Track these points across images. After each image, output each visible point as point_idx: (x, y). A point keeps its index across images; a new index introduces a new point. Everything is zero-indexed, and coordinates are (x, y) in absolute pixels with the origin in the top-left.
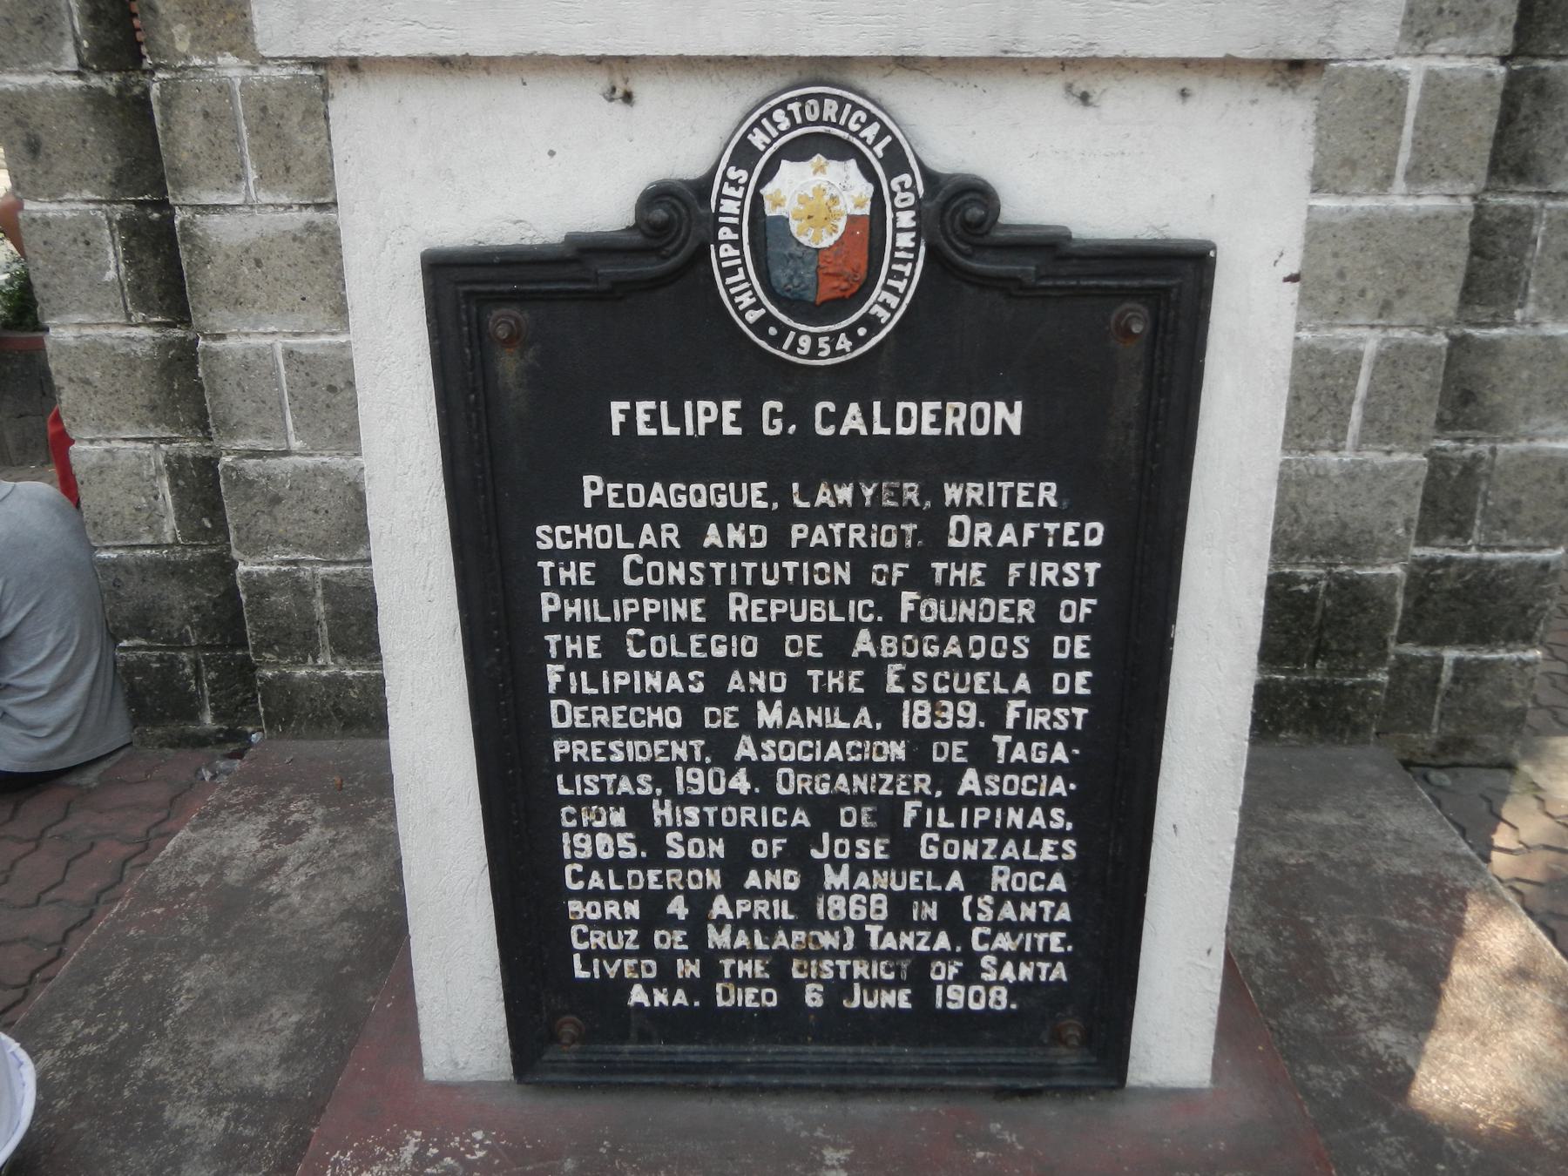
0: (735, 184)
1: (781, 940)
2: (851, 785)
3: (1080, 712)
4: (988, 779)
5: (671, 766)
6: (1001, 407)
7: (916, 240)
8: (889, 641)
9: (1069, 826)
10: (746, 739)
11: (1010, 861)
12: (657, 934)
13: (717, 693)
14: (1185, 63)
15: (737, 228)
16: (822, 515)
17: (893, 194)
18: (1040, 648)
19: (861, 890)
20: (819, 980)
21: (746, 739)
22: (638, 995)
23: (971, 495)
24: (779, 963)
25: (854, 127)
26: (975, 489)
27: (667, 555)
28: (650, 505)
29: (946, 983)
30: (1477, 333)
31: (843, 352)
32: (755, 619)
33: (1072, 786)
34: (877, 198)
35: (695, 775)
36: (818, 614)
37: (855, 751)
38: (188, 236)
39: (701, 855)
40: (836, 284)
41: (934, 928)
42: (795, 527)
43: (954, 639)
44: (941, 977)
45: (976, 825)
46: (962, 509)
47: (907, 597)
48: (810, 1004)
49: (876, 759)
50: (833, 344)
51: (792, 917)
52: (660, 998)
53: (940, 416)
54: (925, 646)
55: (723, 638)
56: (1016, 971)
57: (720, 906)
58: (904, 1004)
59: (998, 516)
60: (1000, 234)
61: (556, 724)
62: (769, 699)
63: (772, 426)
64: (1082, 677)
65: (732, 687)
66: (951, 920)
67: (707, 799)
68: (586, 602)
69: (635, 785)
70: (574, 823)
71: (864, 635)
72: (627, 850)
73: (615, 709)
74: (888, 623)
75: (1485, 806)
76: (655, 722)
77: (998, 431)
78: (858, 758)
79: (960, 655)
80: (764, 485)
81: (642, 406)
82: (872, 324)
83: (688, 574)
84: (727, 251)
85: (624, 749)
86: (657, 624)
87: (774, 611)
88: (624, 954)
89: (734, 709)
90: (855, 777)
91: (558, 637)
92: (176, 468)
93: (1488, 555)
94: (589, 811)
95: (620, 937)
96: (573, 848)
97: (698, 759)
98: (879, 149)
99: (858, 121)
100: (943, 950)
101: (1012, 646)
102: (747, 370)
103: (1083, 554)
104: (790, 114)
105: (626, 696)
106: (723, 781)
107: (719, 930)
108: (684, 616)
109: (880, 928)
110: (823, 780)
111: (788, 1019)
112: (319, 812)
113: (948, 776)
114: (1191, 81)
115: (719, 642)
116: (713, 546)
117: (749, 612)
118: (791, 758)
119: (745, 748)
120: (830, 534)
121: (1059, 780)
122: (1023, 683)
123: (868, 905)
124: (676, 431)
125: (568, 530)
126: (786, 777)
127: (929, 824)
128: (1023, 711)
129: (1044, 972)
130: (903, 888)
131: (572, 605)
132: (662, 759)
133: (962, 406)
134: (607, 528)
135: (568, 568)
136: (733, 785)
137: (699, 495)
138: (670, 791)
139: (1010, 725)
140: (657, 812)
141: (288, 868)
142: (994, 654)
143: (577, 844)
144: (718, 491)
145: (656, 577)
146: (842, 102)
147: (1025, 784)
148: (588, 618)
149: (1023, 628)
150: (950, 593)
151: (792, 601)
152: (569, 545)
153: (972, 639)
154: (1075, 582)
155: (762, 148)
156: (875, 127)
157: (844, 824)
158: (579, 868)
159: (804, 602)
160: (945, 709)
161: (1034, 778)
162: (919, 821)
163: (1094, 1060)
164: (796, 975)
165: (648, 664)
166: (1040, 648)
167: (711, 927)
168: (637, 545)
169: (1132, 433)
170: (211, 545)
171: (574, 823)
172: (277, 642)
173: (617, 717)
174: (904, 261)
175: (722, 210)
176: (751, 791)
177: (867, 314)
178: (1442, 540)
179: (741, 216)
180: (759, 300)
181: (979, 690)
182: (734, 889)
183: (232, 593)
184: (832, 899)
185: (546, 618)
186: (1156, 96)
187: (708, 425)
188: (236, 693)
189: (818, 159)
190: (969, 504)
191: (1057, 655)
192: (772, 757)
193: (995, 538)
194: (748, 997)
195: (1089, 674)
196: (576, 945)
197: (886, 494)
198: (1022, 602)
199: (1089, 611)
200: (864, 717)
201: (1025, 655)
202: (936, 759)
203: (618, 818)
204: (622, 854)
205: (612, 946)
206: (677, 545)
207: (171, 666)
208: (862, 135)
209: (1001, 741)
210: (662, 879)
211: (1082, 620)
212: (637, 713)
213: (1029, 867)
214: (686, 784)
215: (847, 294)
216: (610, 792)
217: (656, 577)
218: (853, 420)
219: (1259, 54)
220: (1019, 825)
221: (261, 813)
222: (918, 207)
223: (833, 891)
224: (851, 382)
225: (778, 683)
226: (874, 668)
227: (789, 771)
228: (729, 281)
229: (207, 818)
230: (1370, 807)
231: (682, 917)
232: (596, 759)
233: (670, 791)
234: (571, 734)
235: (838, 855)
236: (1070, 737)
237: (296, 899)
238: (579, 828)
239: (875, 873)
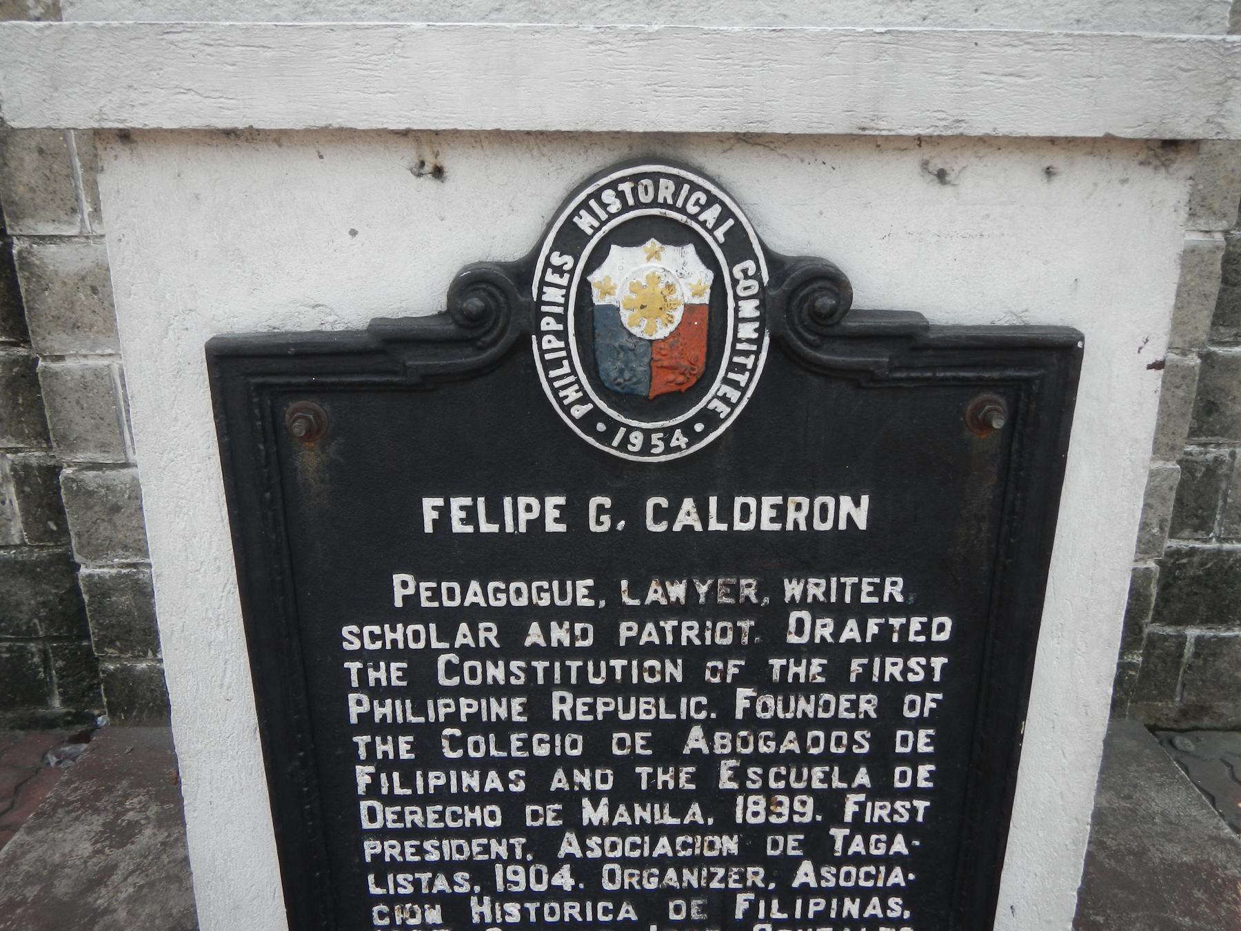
0: (559, 270)
3: (921, 805)
5: (490, 864)
6: (846, 502)
7: (759, 331)
8: (723, 738)
9: (907, 914)
10: (570, 836)
13: (539, 791)
14: (1053, 141)
15: (561, 318)
16: (656, 613)
17: (735, 282)
21: (570, 836)
23: (812, 590)
25: (692, 209)
26: (817, 585)
27: (486, 654)
28: (467, 604)
30: (1220, 351)
31: (678, 448)
32: (580, 717)
33: (911, 876)
34: (718, 288)
35: (516, 873)
36: (648, 712)
37: (685, 846)
38: (26, 265)
40: (671, 377)
42: (624, 625)
43: (791, 735)
45: (811, 915)
46: (802, 604)
47: (743, 695)
49: (707, 853)
50: (667, 441)
54: (761, 742)
55: (546, 737)
59: (840, 612)
60: (851, 324)
61: (366, 825)
63: (599, 523)
64: (924, 770)
65: (555, 785)
67: (528, 895)
68: (398, 703)
69: (452, 883)
71: (696, 732)
73: (429, 809)
74: (722, 716)
75: (1227, 770)
76: (473, 821)
77: (842, 526)
78: (689, 852)
79: (798, 751)
80: (590, 582)
81: (457, 503)
82: (710, 418)
83: (508, 673)
84: (550, 342)
86: (475, 724)
87: (600, 709)
89: (558, 807)
91: (367, 738)
92: (22, 476)
93: (1227, 546)
94: (403, 909)
97: (519, 854)
98: (720, 233)
99: (697, 203)
101: (852, 741)
102: (571, 465)
103: (929, 649)
106: (545, 877)
108: (504, 715)
110: (651, 875)
112: (154, 809)
113: (783, 868)
114: (1058, 160)
115: (541, 741)
116: (535, 645)
117: (573, 710)
118: (618, 854)
119: (570, 846)
120: (661, 632)
121: (898, 871)
122: (862, 778)
124: (495, 528)
125: (377, 630)
127: (761, 915)
128: (862, 805)
131: (382, 705)
132: (480, 857)
133: (805, 502)
134: (420, 627)
135: (377, 669)
136: (556, 881)
137: (519, 594)
138: (488, 888)
139: (848, 818)
141: (117, 878)
142: (833, 749)
144: (540, 589)
146: (679, 182)
147: (862, 875)
148: (400, 719)
149: (866, 722)
150: (787, 689)
151: (620, 700)
152: (378, 645)
153: (811, 734)
154: (920, 677)
155: (589, 231)
156: (716, 210)
159: (633, 700)
160: (780, 804)
165: (466, 764)
168: (452, 645)
169: (984, 526)
170: (57, 546)
172: (118, 638)
173: (431, 817)
174: (746, 354)
175: (545, 298)
177: (705, 408)
178: (1187, 533)
179: (565, 305)
180: (585, 393)
181: (816, 785)
183: (75, 591)
185: (354, 720)
186: (1020, 176)
188: (83, 679)
189: (652, 244)
190: (810, 600)
191: (899, 749)
192: (597, 853)
193: (837, 634)
195: (932, 767)
197: (721, 590)
198: (863, 698)
199: (934, 705)
200: (695, 813)
201: (866, 750)
202: (770, 852)
206: (496, 644)
207: (20, 656)
208: (702, 218)
209: (839, 834)
211: (926, 714)
212: (454, 813)
214: (506, 881)
215: (684, 388)
216: (425, 891)
218: (687, 515)
219: (1142, 133)
220: (855, 915)
221: (97, 811)
222: (762, 295)
224: (685, 478)
226: (707, 765)
227: (616, 867)
228: (553, 374)
229: (45, 817)
230: (1135, 786)
232: (409, 858)
233: (488, 888)
234: (383, 834)
236: (909, 830)
237: (122, 915)
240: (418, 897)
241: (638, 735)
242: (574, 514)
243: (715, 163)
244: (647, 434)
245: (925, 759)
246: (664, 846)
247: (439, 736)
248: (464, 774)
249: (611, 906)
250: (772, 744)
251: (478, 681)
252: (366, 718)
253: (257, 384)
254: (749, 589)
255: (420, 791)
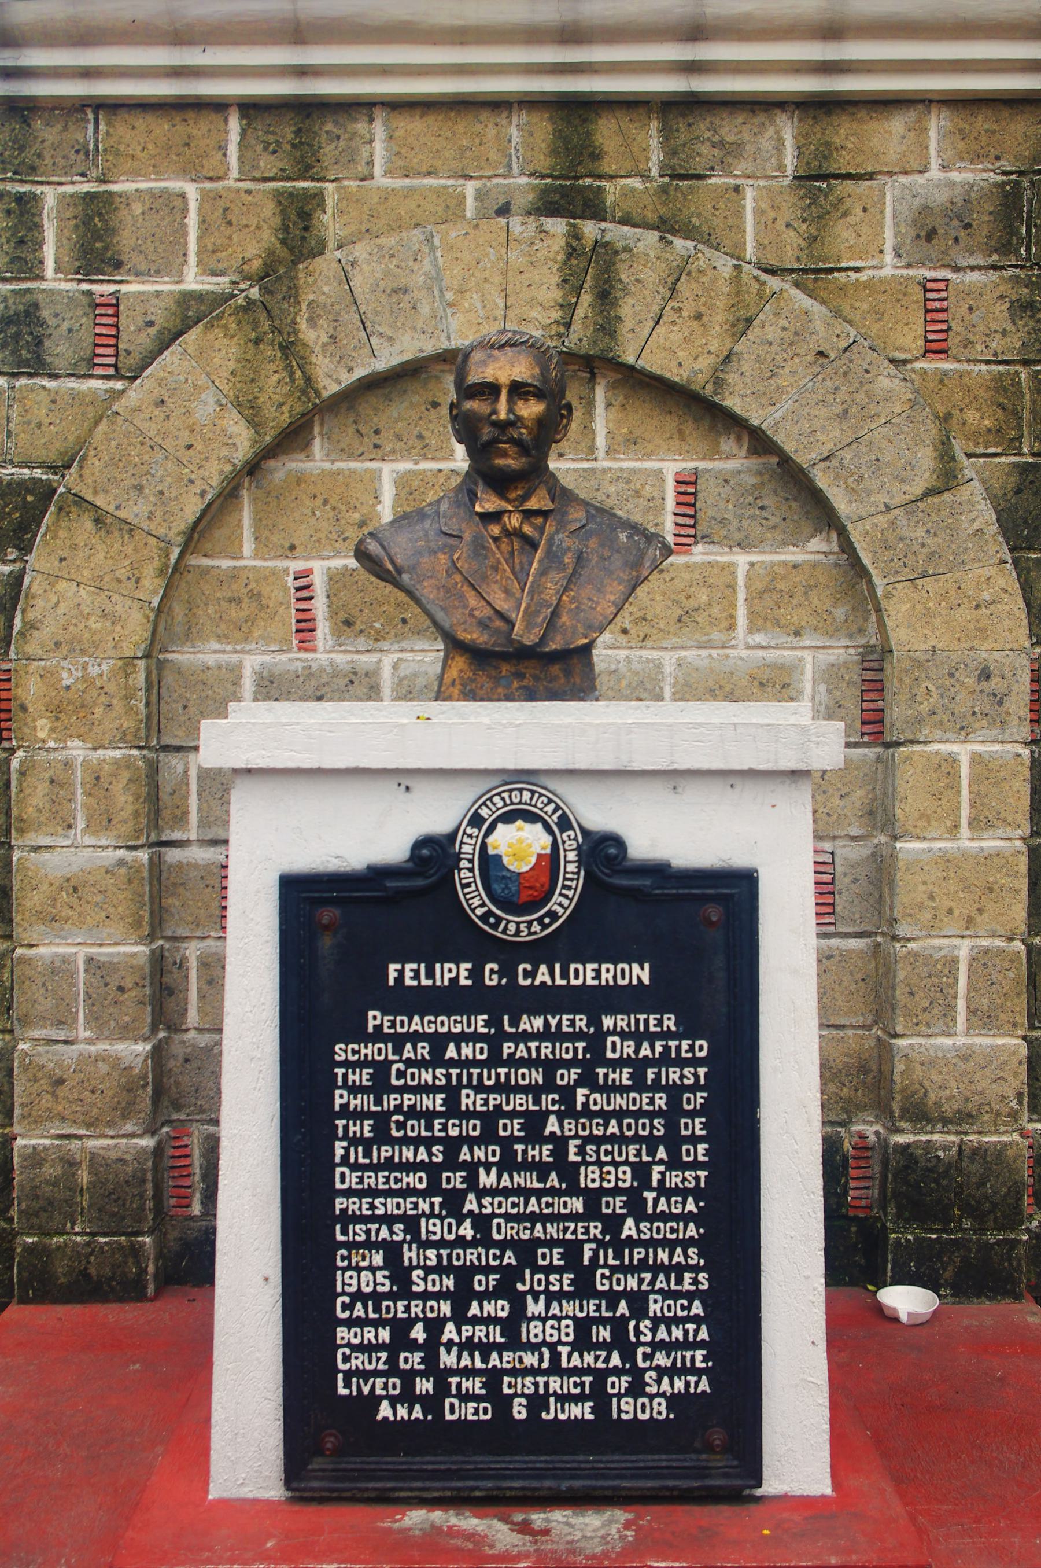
0: (470, 836)
1: (494, 1360)
2: (545, 1232)
3: (703, 1174)
4: (642, 1225)
5: (418, 1217)
6: (636, 967)
7: (578, 867)
9: (702, 1262)
10: (471, 1196)
11: (661, 1291)
12: (402, 1355)
13: (451, 1163)
15: (471, 861)
16: (526, 1037)
17: (564, 842)
18: (672, 1127)
19: (554, 1317)
20: (523, 1395)
21: (471, 1196)
22: (385, 1411)
23: (619, 1023)
24: (493, 1378)
25: (540, 805)
29: (619, 1396)
31: (535, 933)
32: (479, 1108)
33: (702, 1231)
34: (555, 845)
35: (434, 1225)
39: (437, 1289)
41: (608, 1347)
42: (506, 1045)
43: (613, 1122)
44: (616, 1391)
45: (635, 1262)
46: (614, 1033)
47: (581, 1092)
48: (517, 1416)
49: (563, 1211)
50: (529, 928)
51: (503, 1340)
52: (402, 1412)
53: (598, 972)
55: (457, 1122)
56: (672, 1385)
57: (450, 1332)
58: (589, 1417)
59: (638, 1037)
60: (628, 864)
61: (338, 1186)
62: (488, 1166)
63: (491, 979)
64: (701, 1148)
65: (462, 1157)
66: (621, 1343)
67: (442, 1243)
69: (392, 1233)
70: (346, 1263)
71: (553, 1119)
72: (383, 1285)
73: (380, 1174)
74: (568, 1111)
76: (408, 1184)
77: (635, 982)
80: (485, 1017)
81: (409, 966)
82: (553, 916)
83: (435, 1077)
84: (465, 873)
85: (385, 1205)
86: (413, 1113)
87: (491, 1103)
88: (376, 1373)
89: (464, 1174)
90: (548, 1225)
95: (374, 1360)
96: (343, 1284)
98: (555, 817)
100: (616, 1367)
101: (652, 1127)
102: (476, 944)
103: (695, 1062)
104: (503, 799)
105: (389, 1165)
106: (454, 1228)
107: (449, 1352)
109: (568, 1349)
110: (525, 1228)
111: (500, 1434)
113: (613, 1224)
115: (454, 1125)
116: (451, 1059)
117: (474, 1103)
118: (503, 1211)
119: (471, 1204)
120: (529, 1049)
121: (692, 1225)
122: (661, 1153)
123: (559, 1329)
124: (430, 982)
125: (356, 1047)
126: (499, 1225)
127: (602, 1262)
128: (663, 1174)
129: (692, 1385)
130: (584, 1314)
131: (355, 1098)
133: (611, 967)
134: (382, 1046)
135: (354, 1073)
136: (461, 1232)
139: (655, 1184)
140: (407, 1255)
142: (641, 1133)
143: (347, 1281)
144: (455, 1021)
145: (413, 1079)
146: (533, 792)
148: (366, 1108)
149: (659, 1113)
150: (610, 1089)
152: (356, 1057)
153: (626, 1121)
154: (692, 1081)
156: (552, 806)
157: (541, 1262)
158: (347, 1299)
161: (674, 1224)
162: (595, 1258)
163: (735, 1463)
164: (506, 1391)
165: (405, 1141)
166: (672, 1127)
167: (442, 1349)
171: (346, 1263)
173: (381, 1180)
174: (572, 880)
176: (474, 1237)
177: (549, 911)
181: (632, 1159)
182: (460, 1318)
184: (533, 1324)
185: (337, 1108)
187: (450, 979)
189: (520, 823)
191: (684, 1133)
193: (637, 1051)
194: (469, 1411)
195: (706, 1146)
196: (341, 1366)
197: (565, 1023)
198: (657, 1096)
201: (662, 1133)
203: (378, 1259)
204: (379, 1289)
205: (368, 1367)
206: (427, 1057)
209: (650, 1196)
210: (407, 1309)
212: (396, 1178)
213: (676, 1295)
214: (428, 1231)
216: (373, 1238)
217: (413, 1079)
218: (543, 975)
222: (579, 848)
223: (533, 1318)
225: (494, 1154)
226: (560, 1143)
227: (502, 1221)
228: (466, 890)
231: (421, 1341)
234: (349, 1193)
235: (536, 1288)
236: (697, 1193)
238: (349, 1267)
239: (564, 1302)
240: (369, 1245)
241: (515, 1121)
242: (476, 973)
243: (552, 784)
244: (518, 924)
245: (701, 1139)
246: (533, 1206)
247: (390, 1120)
248: (404, 1148)
249: (498, 1253)
250: (601, 1128)
251: (415, 1083)
252: (345, 1106)
253: (306, 899)
254: (581, 1022)
255: (375, 1161)
